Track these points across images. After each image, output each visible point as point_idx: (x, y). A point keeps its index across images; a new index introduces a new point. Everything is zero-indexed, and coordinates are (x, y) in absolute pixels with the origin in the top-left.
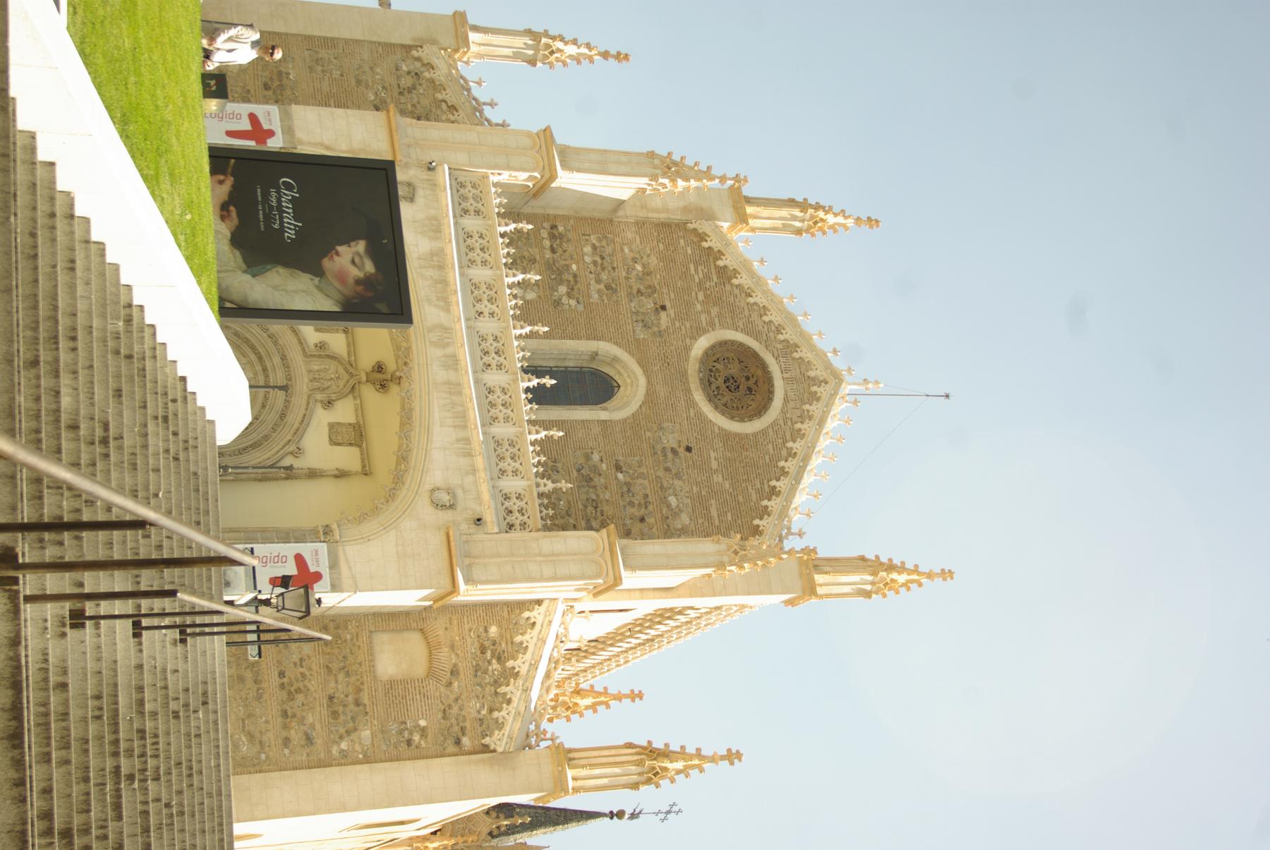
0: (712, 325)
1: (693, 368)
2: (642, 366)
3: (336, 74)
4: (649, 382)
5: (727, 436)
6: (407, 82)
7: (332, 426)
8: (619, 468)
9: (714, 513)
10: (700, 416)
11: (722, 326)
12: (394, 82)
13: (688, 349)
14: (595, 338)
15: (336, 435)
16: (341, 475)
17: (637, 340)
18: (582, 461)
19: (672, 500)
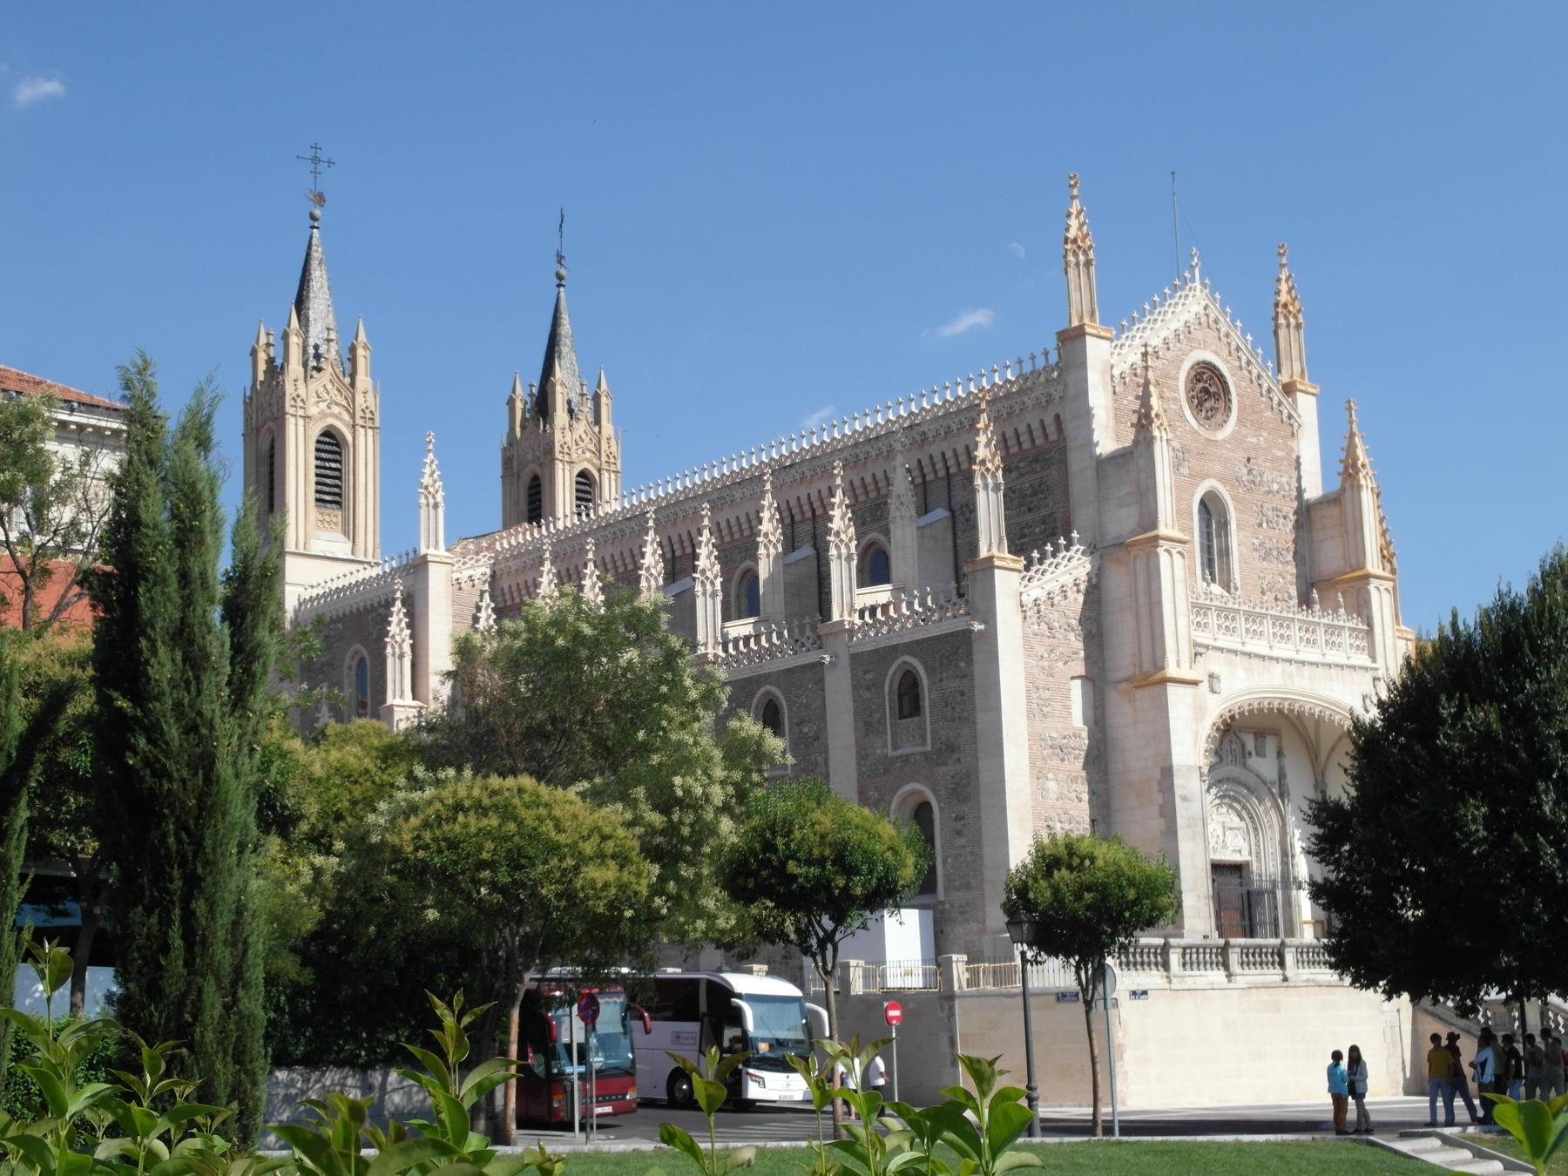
0: (1176, 400)
1: (1202, 431)
2: (1203, 479)
3: (1047, 694)
4: (1214, 476)
5: (1241, 421)
6: (1044, 627)
7: (1258, 754)
8: (1260, 525)
9: (1280, 454)
10: (1232, 438)
11: (1176, 391)
12: (1048, 641)
13: (1194, 432)
14: (1191, 514)
15: (1261, 753)
16: (1280, 754)
17: (1191, 476)
18: (1256, 555)
19: (1275, 487)
